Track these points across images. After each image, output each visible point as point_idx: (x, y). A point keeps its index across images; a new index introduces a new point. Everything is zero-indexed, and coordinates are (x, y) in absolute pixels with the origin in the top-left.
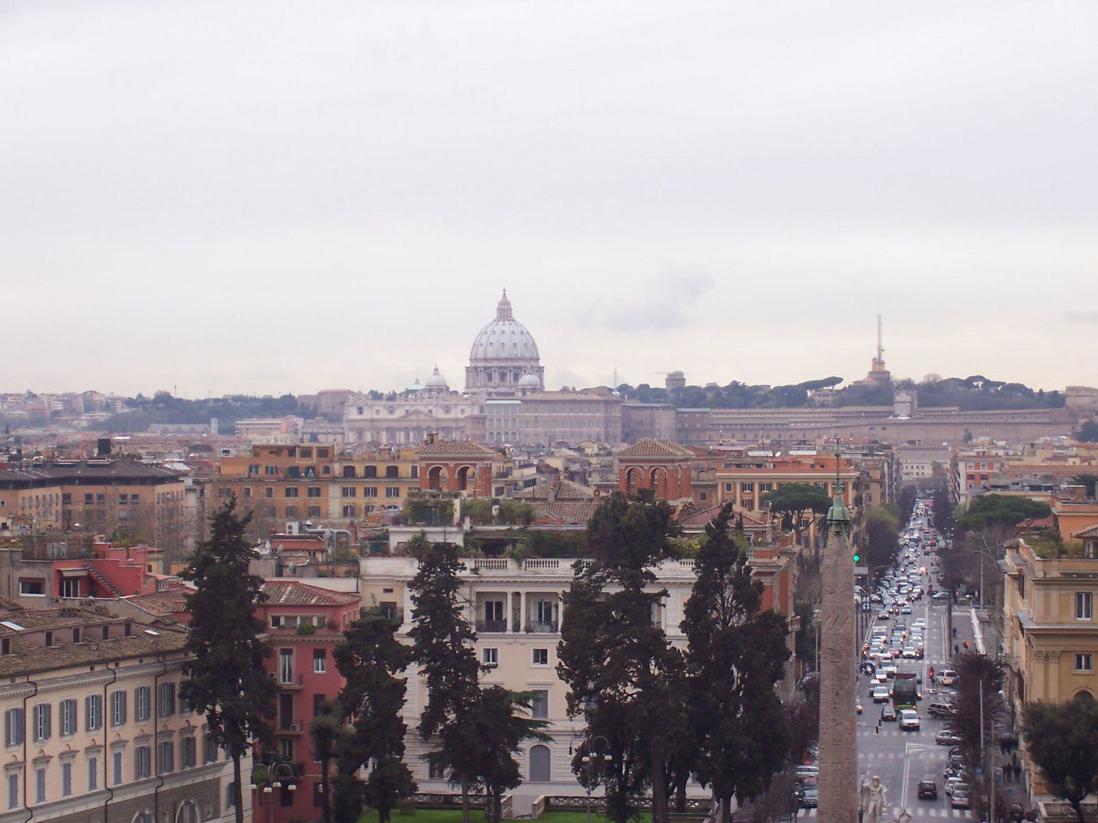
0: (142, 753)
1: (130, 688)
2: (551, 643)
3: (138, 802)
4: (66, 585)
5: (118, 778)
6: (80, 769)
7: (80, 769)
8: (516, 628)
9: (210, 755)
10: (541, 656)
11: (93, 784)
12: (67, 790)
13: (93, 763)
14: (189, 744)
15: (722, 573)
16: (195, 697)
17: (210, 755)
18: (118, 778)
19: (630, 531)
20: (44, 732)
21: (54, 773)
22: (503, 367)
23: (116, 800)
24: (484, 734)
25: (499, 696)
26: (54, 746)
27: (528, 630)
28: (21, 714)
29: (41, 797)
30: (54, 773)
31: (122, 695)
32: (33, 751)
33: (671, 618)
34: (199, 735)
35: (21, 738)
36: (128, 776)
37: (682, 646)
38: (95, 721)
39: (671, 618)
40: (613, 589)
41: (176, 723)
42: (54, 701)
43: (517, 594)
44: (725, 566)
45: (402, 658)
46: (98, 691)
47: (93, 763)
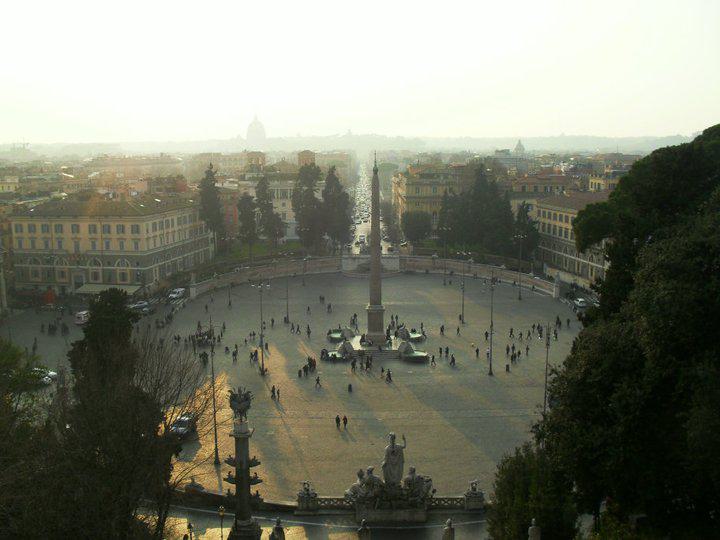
1: (187, 215)
2: (289, 204)
4: (168, 190)
6: (176, 234)
7: (176, 234)
9: (206, 231)
10: (284, 205)
16: (202, 218)
17: (206, 231)
20: (168, 227)
21: (170, 237)
22: (520, 146)
24: (275, 225)
25: (277, 214)
30: (170, 237)
32: (165, 231)
33: (318, 195)
35: (162, 228)
36: (187, 237)
38: (178, 224)
39: (318, 195)
40: (305, 188)
41: (198, 223)
45: (254, 206)
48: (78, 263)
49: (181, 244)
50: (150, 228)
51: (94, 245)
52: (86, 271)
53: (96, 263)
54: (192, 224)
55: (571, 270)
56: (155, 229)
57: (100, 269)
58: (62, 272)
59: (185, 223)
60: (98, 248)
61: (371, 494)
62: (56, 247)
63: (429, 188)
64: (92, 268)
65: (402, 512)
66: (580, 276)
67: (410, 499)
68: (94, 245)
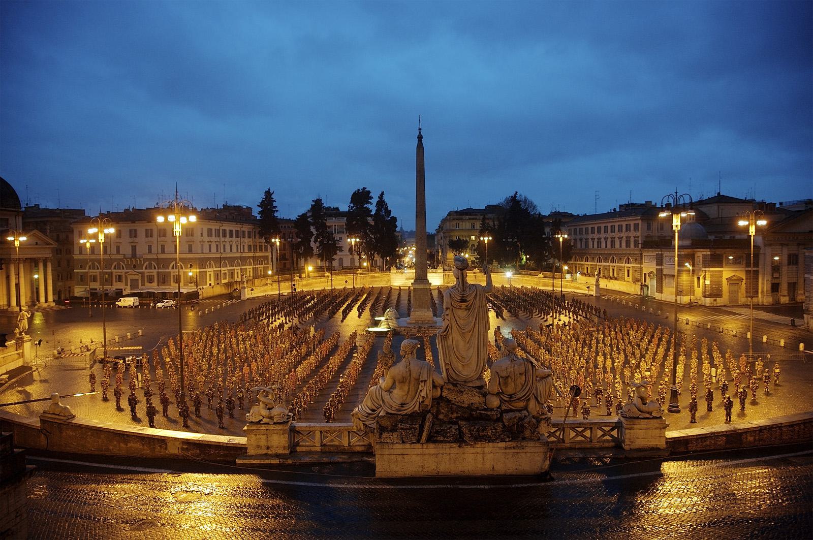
0: (249, 246)
3: (249, 257)
5: (244, 251)
8: (335, 233)
11: (237, 251)
12: (231, 251)
13: (237, 246)
14: (261, 246)
15: (382, 208)
18: (244, 251)
19: (361, 197)
23: (244, 255)
26: (228, 239)
27: (338, 233)
28: (219, 230)
29: (224, 251)
31: (244, 232)
34: (263, 244)
35: (219, 236)
36: (246, 250)
37: (373, 224)
42: (228, 229)
43: (335, 225)
44: (382, 206)
45: (310, 224)
46: (239, 229)
47: (237, 246)
48: (135, 266)
49: (238, 255)
50: (205, 234)
51: (150, 247)
52: (142, 273)
53: (149, 267)
54: (250, 240)
55: (606, 274)
56: (210, 235)
57: (154, 272)
58: (120, 276)
59: (244, 237)
60: (154, 250)
61: (413, 406)
62: (114, 251)
63: (467, 223)
64: (147, 272)
65: (489, 447)
66: (616, 279)
67: (506, 417)
68: (150, 247)
